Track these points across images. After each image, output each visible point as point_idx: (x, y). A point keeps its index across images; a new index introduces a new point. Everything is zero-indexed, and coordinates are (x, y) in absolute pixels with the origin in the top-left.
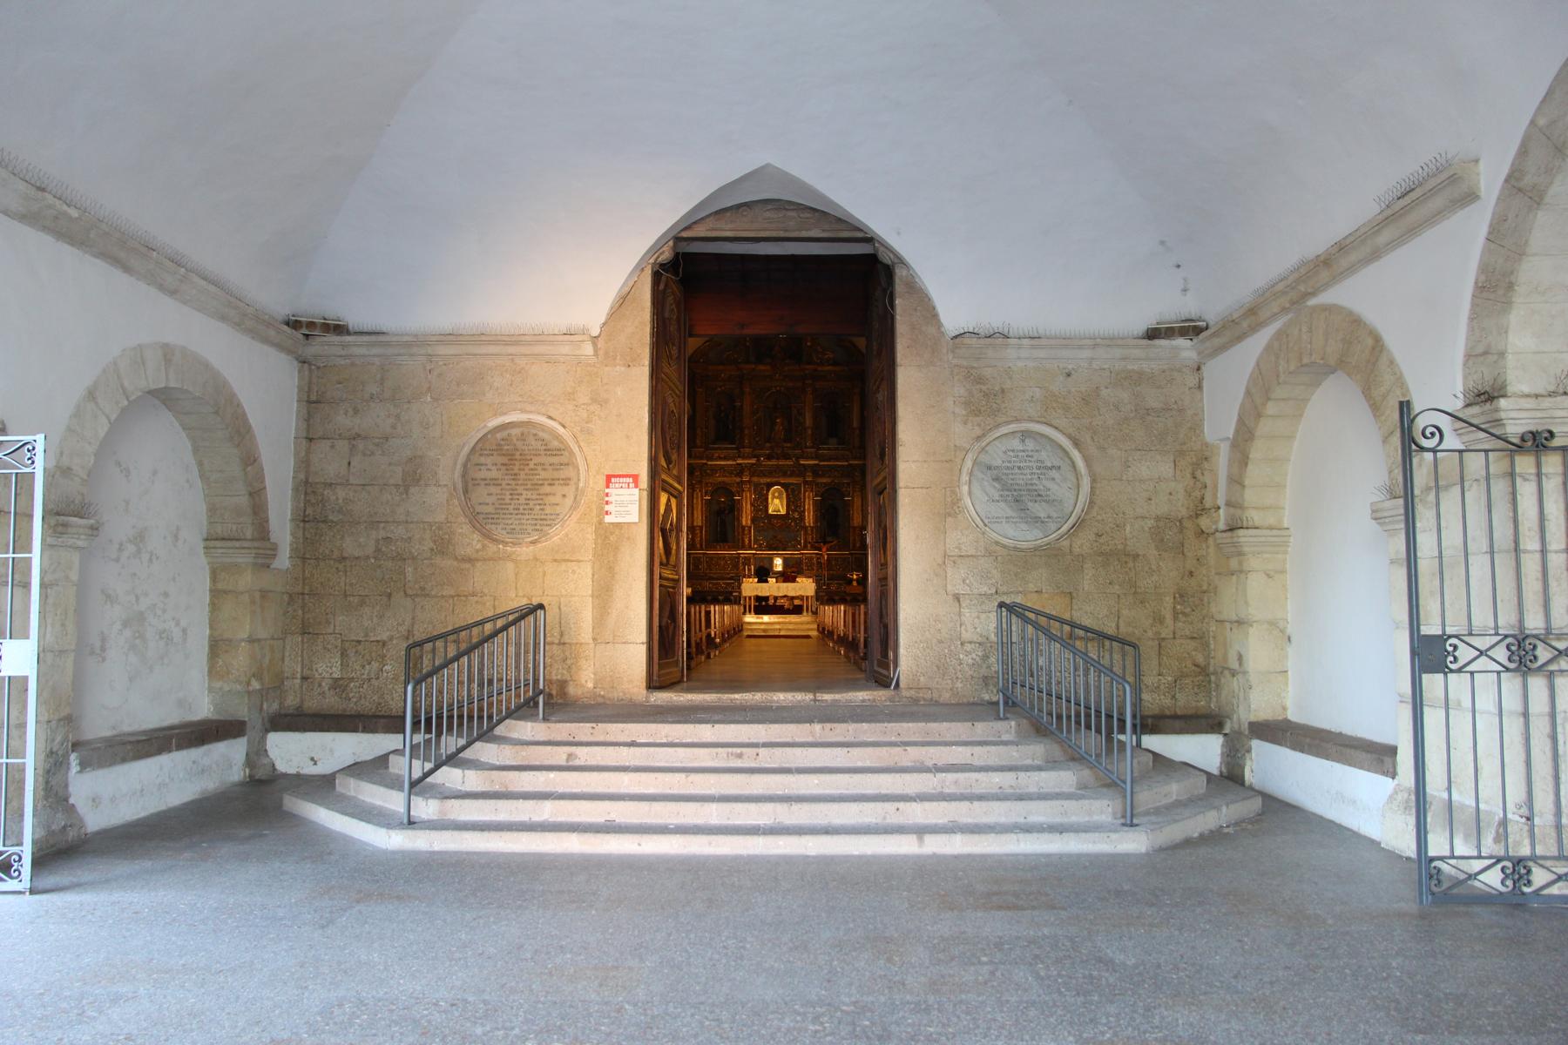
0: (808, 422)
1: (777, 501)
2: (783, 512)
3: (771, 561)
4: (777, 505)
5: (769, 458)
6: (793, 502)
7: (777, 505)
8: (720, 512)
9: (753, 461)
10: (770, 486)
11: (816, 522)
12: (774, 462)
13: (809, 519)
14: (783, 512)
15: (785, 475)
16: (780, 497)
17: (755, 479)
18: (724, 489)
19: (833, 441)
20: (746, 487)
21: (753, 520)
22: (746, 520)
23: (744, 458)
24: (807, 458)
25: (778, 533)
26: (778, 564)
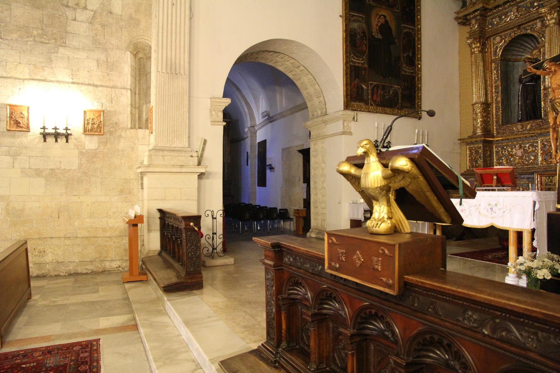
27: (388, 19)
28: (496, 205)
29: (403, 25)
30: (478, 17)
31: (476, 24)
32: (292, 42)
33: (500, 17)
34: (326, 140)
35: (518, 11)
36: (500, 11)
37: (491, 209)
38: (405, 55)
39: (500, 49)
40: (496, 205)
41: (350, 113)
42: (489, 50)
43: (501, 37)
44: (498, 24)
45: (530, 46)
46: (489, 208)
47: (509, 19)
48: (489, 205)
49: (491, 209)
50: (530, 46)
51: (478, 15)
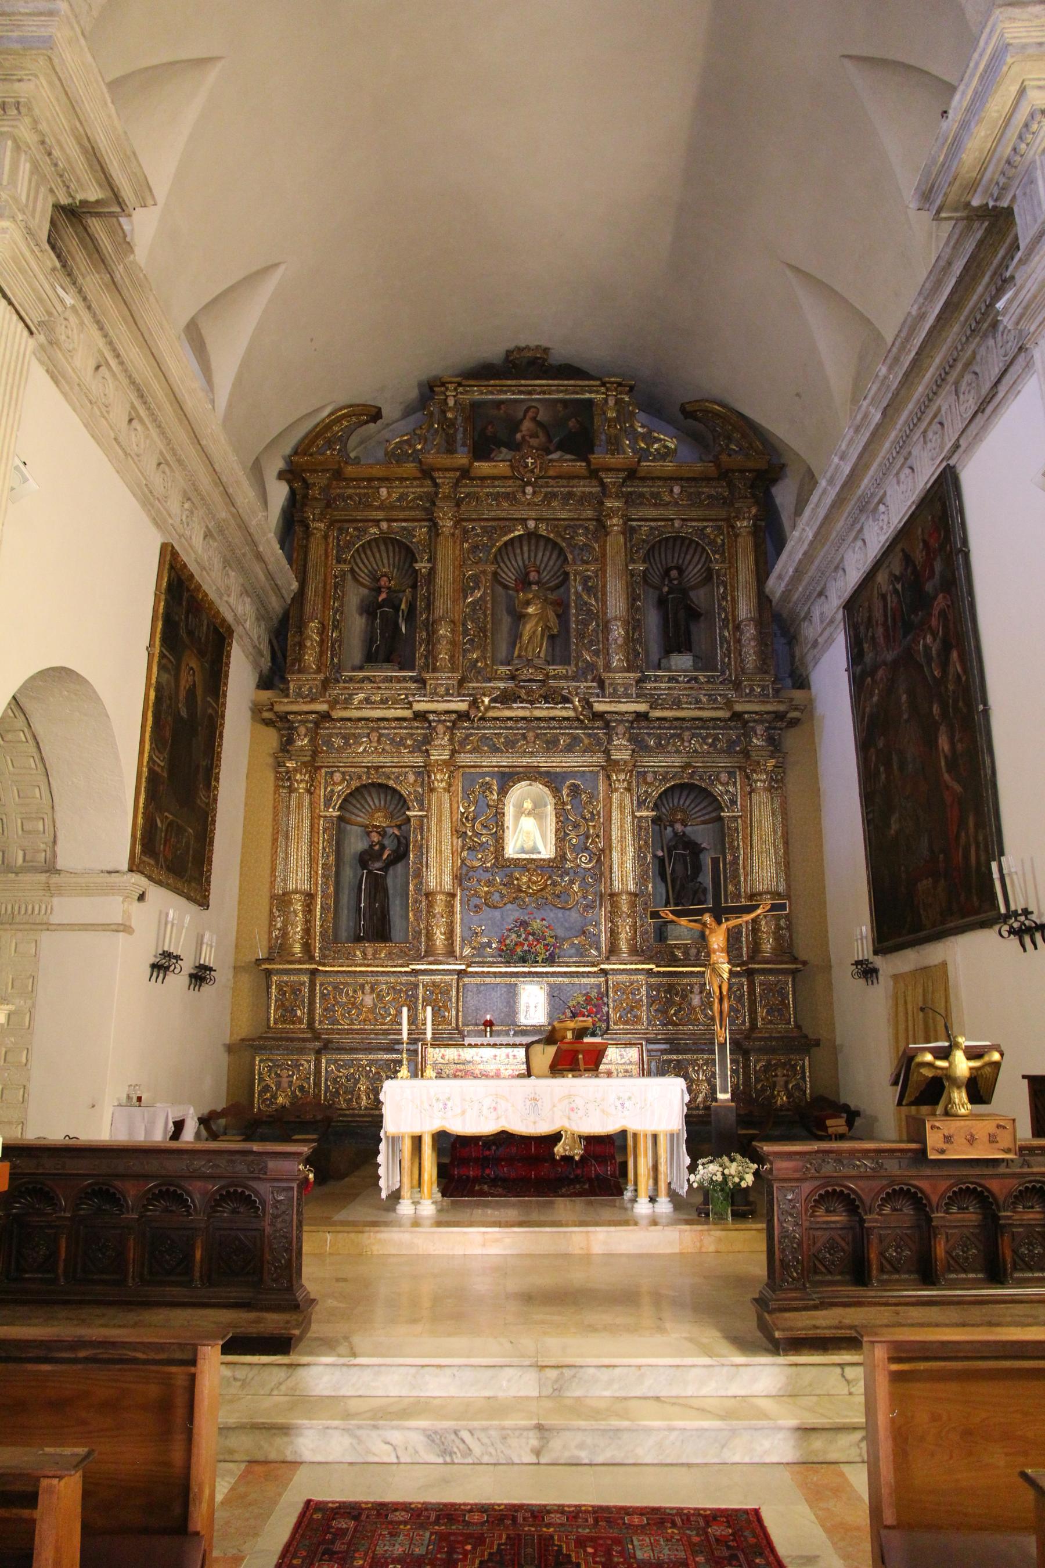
0: (616, 603)
1: (528, 823)
2: (547, 851)
3: (512, 994)
4: (529, 830)
5: (505, 699)
6: (577, 820)
7: (529, 830)
8: (364, 859)
9: (463, 706)
10: (507, 779)
11: (641, 879)
12: (518, 711)
13: (625, 868)
14: (547, 851)
15: (551, 745)
16: (535, 811)
17: (465, 759)
18: (381, 790)
19: (682, 661)
20: (440, 780)
21: (459, 878)
22: (439, 872)
23: (434, 695)
24: (615, 697)
25: (532, 917)
26: (533, 1004)
27: (196, 679)
28: (630, 1098)
29: (209, 699)
30: (310, 725)
31: (305, 736)
32: (86, 681)
33: (346, 738)
34: (45, 937)
35: (379, 741)
36: (346, 728)
37: (622, 1105)
38: (204, 764)
39: (339, 796)
40: (630, 1098)
41: (139, 881)
42: (317, 791)
43: (343, 773)
44: (340, 750)
45: (371, 803)
46: (618, 1103)
47: (361, 749)
48: (619, 1099)
49: (622, 1105)
50: (371, 803)
51: (311, 722)
